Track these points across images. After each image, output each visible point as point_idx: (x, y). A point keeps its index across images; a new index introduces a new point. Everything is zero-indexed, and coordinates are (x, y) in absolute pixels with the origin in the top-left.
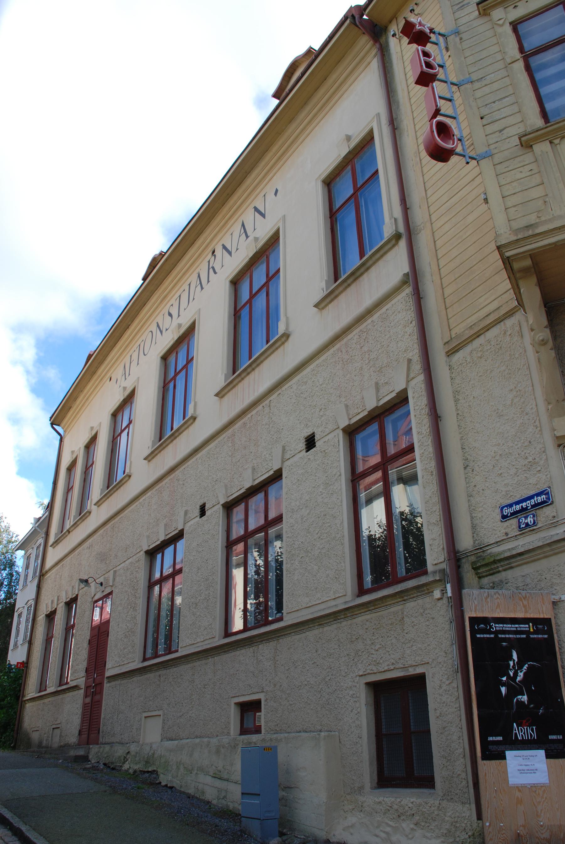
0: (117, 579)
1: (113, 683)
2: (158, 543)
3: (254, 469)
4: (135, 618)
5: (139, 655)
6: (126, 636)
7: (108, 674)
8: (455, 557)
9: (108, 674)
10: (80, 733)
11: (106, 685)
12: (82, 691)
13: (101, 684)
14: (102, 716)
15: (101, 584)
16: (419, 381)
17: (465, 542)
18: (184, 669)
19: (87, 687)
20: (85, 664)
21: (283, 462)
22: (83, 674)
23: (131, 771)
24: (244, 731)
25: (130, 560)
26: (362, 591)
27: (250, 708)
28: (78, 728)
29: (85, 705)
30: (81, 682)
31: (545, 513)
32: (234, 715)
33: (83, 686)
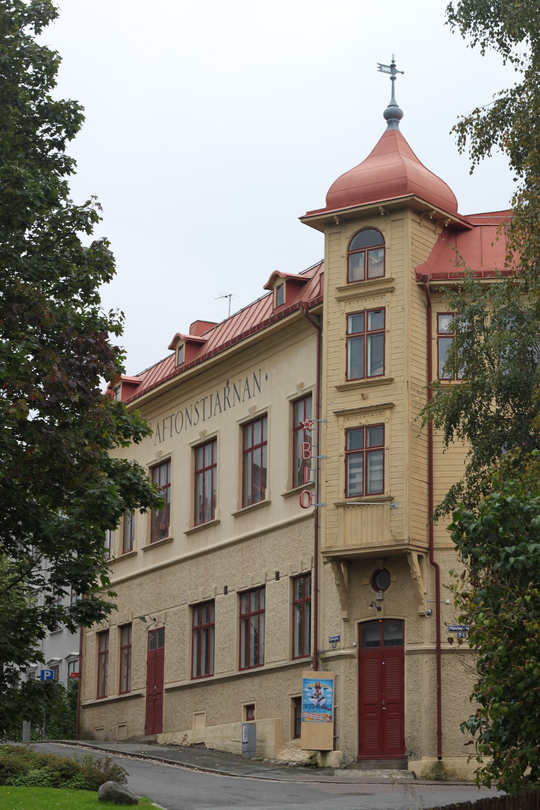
0: (168, 619)
1: (170, 694)
2: (198, 602)
3: (252, 578)
4: (184, 650)
5: (188, 676)
6: (178, 662)
7: (166, 686)
8: (317, 653)
9: (166, 686)
10: (146, 728)
11: (165, 695)
12: (145, 699)
13: (161, 694)
14: (164, 715)
15: (155, 620)
16: (313, 570)
17: (320, 648)
18: (218, 688)
19: (148, 695)
20: (145, 678)
21: (266, 581)
22: (144, 685)
23: (189, 745)
24: (248, 719)
25: (178, 608)
26: (294, 658)
27: (250, 708)
28: (144, 724)
29: (148, 708)
30: (144, 692)
31: (338, 644)
32: (243, 712)
33: (145, 695)
